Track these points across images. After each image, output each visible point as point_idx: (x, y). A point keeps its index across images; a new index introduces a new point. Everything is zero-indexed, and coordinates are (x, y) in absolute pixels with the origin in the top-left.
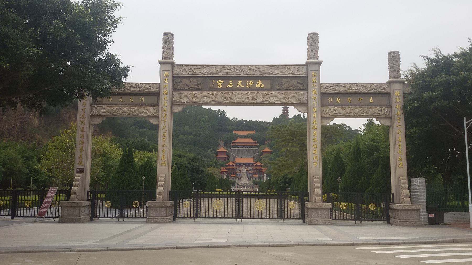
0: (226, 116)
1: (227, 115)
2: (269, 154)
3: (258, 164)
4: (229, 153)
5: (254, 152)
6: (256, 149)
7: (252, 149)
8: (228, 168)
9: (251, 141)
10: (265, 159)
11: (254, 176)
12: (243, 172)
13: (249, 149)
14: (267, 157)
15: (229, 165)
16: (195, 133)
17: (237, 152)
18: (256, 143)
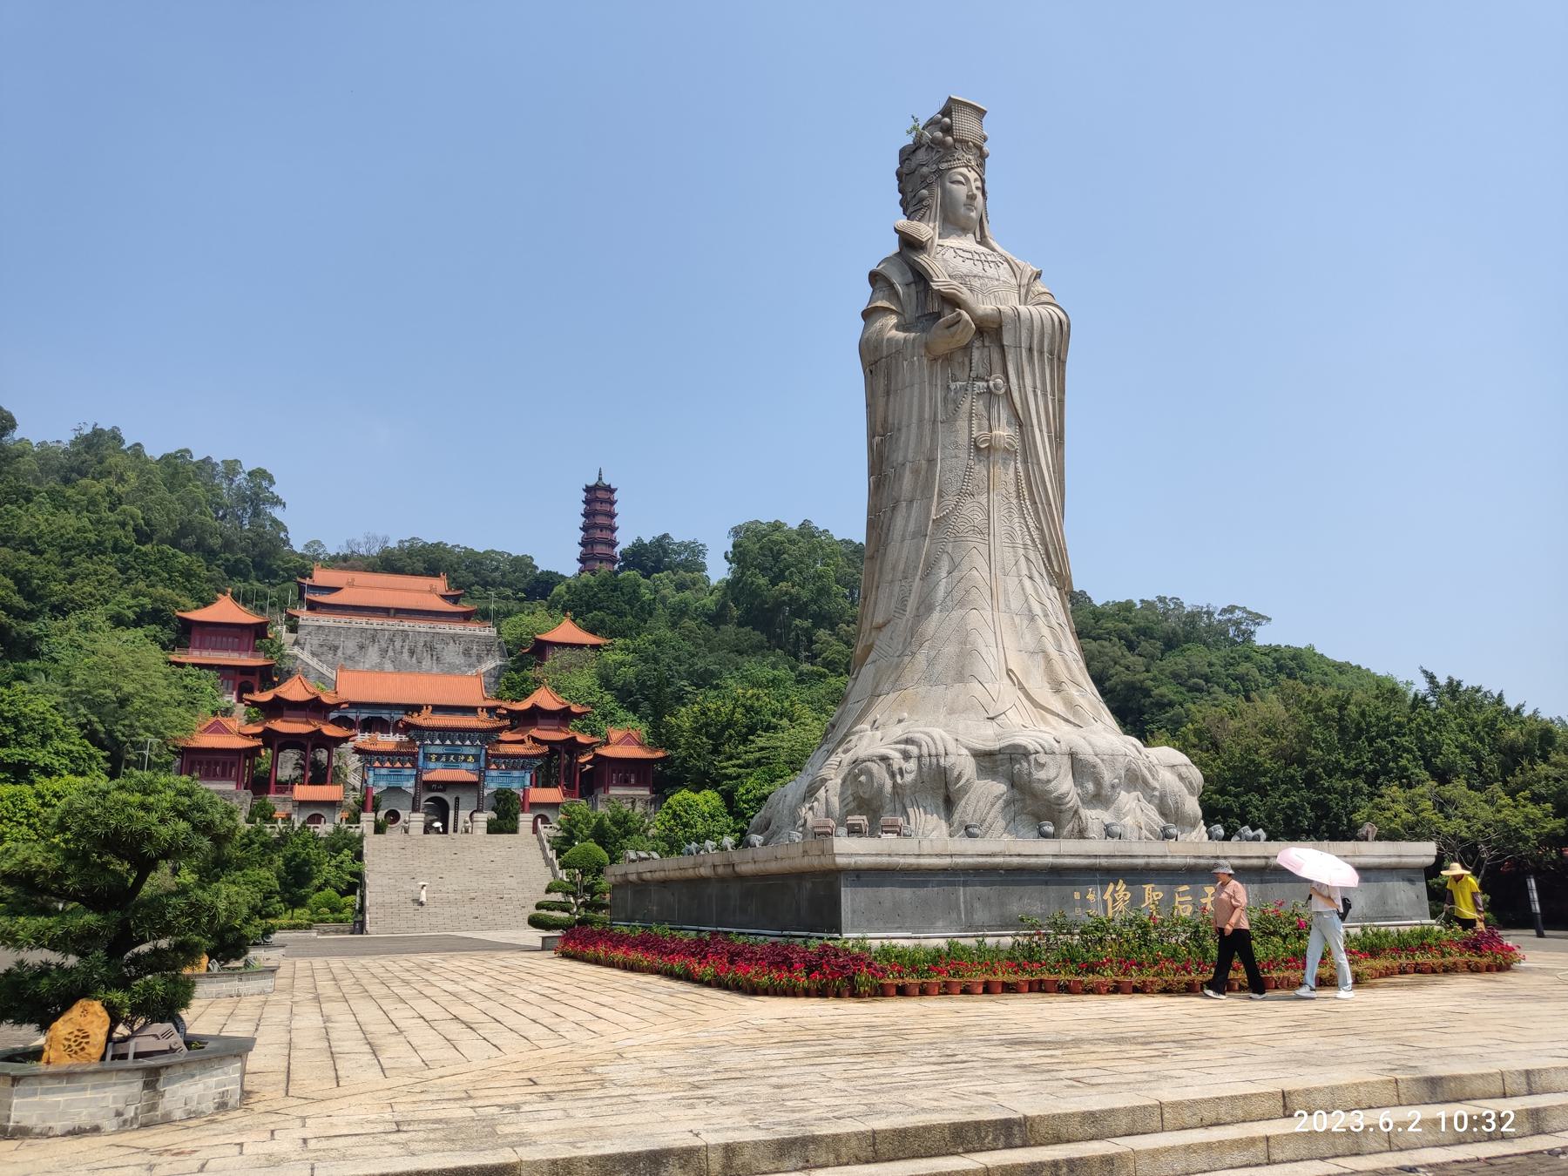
3: (545, 698)
5: (467, 653)
7: (454, 638)
12: (990, 330)
15: (278, 707)
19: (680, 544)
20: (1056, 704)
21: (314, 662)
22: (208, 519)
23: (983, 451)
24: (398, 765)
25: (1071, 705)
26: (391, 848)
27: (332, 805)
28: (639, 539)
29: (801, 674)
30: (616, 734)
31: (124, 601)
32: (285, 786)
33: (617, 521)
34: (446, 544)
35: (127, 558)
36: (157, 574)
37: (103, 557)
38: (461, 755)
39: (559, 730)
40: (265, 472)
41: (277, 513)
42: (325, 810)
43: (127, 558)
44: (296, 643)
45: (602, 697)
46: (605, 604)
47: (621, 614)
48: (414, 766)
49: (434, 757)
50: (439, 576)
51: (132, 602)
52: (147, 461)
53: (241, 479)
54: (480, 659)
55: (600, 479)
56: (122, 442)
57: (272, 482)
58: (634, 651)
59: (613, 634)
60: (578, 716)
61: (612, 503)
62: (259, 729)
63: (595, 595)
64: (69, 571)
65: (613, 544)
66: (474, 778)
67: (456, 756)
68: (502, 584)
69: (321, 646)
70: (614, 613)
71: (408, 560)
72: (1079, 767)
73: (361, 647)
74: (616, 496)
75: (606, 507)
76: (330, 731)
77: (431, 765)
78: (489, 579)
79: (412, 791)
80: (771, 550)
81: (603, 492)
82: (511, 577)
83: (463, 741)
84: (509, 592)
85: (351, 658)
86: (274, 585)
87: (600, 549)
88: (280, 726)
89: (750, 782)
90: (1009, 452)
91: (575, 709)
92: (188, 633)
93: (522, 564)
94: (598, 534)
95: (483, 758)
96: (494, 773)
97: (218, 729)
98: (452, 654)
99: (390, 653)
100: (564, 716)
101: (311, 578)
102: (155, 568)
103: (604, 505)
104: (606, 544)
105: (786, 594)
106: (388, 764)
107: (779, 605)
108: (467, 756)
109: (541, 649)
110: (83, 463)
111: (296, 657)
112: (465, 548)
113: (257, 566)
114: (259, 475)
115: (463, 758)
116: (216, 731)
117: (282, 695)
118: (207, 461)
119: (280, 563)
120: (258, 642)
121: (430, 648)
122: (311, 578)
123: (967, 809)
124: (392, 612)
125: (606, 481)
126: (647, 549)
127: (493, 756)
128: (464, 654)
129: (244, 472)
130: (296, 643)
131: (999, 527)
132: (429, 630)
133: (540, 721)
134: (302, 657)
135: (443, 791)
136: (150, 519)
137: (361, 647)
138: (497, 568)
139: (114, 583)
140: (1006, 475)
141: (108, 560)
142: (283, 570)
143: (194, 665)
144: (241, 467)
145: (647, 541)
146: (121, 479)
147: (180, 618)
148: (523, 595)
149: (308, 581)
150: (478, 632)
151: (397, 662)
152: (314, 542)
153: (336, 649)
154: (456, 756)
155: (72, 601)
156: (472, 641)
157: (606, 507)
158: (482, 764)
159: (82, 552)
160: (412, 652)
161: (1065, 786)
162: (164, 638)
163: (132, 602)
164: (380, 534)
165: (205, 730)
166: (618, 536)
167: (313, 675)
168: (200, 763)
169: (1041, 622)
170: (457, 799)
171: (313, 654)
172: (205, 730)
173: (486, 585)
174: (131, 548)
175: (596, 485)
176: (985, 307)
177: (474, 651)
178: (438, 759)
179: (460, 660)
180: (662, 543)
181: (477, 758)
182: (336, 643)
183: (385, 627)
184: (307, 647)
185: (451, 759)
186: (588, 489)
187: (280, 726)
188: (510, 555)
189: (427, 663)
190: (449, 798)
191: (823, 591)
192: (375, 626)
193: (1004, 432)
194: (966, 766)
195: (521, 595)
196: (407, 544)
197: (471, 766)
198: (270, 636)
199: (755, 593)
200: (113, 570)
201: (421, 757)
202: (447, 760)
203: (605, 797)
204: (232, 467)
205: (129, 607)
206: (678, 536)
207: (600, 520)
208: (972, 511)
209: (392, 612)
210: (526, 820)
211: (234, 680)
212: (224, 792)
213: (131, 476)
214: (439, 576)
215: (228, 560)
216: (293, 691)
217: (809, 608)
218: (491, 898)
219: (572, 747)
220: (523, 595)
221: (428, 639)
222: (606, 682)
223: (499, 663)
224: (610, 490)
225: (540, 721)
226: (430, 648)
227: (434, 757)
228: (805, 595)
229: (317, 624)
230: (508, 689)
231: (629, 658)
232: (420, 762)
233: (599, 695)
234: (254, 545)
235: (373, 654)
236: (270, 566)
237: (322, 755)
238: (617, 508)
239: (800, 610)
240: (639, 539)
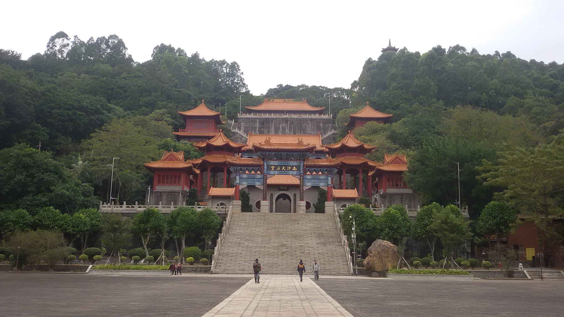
0: (241, 75)
1: (242, 73)
2: (382, 125)
4: (230, 130)
6: (326, 119)
7: (312, 120)
8: (204, 162)
9: (306, 107)
10: (367, 138)
13: (301, 120)
14: (375, 132)
15: (210, 149)
16: (124, 75)
17: (260, 128)
18: (320, 113)
24: (253, 172)
26: (245, 220)
38: (289, 166)
42: (226, 201)
48: (262, 173)
49: (273, 167)
52: (186, 57)
55: (390, 44)
56: (173, 49)
62: (200, 161)
66: (296, 181)
67: (286, 167)
77: (272, 172)
83: (317, 172)
95: (302, 168)
96: (309, 177)
100: (360, 150)
106: (247, 172)
108: (292, 167)
115: (290, 168)
125: (393, 45)
127: (307, 167)
134: (239, 133)
135: (287, 190)
147: (181, 115)
154: (286, 167)
158: (302, 172)
170: (295, 195)
178: (275, 169)
181: (298, 167)
185: (284, 170)
190: (290, 194)
197: (295, 173)
201: (265, 167)
202: (281, 169)
210: (329, 205)
218: (296, 253)
219: (366, 168)
227: (273, 167)
232: (265, 171)
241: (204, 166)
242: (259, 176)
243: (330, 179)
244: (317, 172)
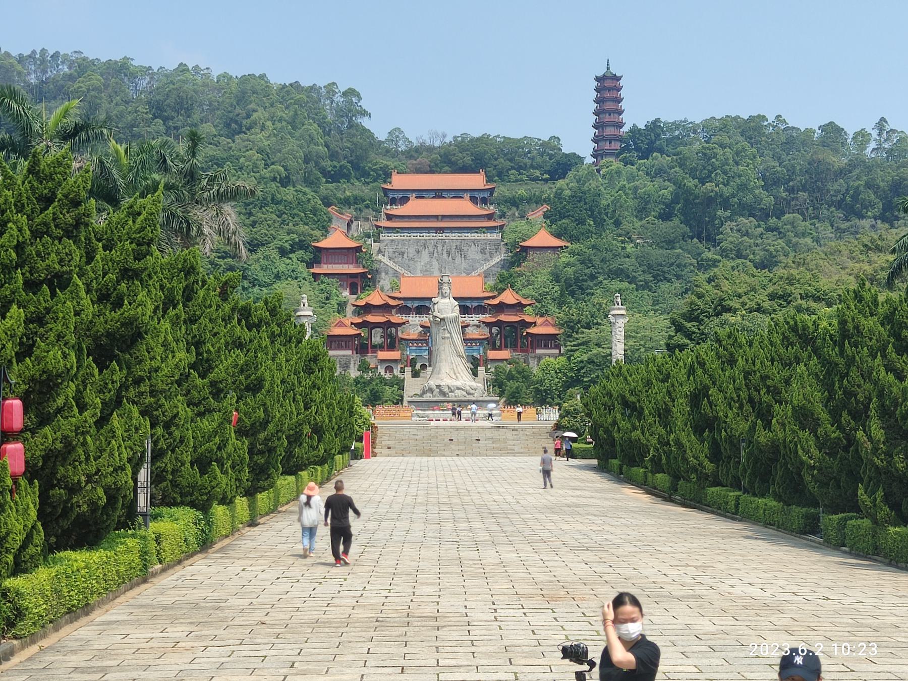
3: (509, 297)
5: (483, 251)
11: (492, 354)
12: (443, 319)
15: (368, 308)
19: (673, 124)
20: (455, 377)
21: (390, 264)
22: (321, 148)
23: (443, 338)
25: (457, 377)
27: (395, 361)
28: (634, 126)
29: (702, 260)
30: (539, 320)
31: (284, 239)
32: (376, 348)
33: (623, 105)
34: (489, 135)
35: (281, 207)
36: (298, 215)
37: (268, 208)
39: (516, 315)
40: (354, 90)
41: (365, 122)
43: (281, 207)
44: (380, 251)
45: (553, 288)
46: (571, 213)
47: (581, 222)
50: (479, 172)
51: (288, 238)
53: (338, 98)
54: (491, 255)
55: (608, 69)
57: (360, 98)
58: (578, 254)
59: (573, 239)
60: (529, 305)
61: (619, 89)
63: (564, 207)
64: (252, 218)
65: (620, 125)
68: (532, 167)
69: (394, 252)
70: (576, 220)
71: (460, 155)
72: (449, 388)
73: (418, 252)
74: (622, 82)
75: (613, 94)
76: (396, 318)
78: (522, 164)
79: (427, 357)
80: (705, 154)
81: (610, 81)
82: (538, 159)
84: (537, 173)
85: (412, 259)
86: (368, 183)
87: (609, 131)
88: (371, 318)
89: (577, 354)
90: (448, 338)
91: (524, 302)
92: (318, 256)
93: (550, 147)
94: (607, 118)
97: (341, 324)
98: (473, 253)
99: (436, 254)
100: (519, 307)
101: (390, 183)
102: (296, 211)
103: (611, 92)
104: (614, 126)
105: (712, 191)
107: (709, 201)
109: (525, 249)
110: (238, 115)
111: (380, 261)
112: (504, 137)
113: (356, 166)
114: (350, 93)
116: (340, 326)
117: (369, 302)
118: (312, 88)
119: (370, 165)
120: (358, 254)
121: (459, 250)
122: (390, 183)
123: (434, 393)
124: (440, 218)
125: (613, 70)
126: (641, 134)
128: (481, 253)
129: (340, 91)
130: (380, 251)
131: (447, 349)
132: (458, 238)
133: (505, 310)
134: (383, 261)
136: (287, 166)
137: (418, 252)
138: (529, 152)
139: (276, 225)
140: (448, 341)
141: (271, 210)
142: (373, 170)
143: (325, 274)
144: (337, 88)
145: (642, 126)
146: (263, 128)
147: (314, 246)
148: (547, 176)
149: (388, 186)
150: (489, 237)
151: (440, 261)
152: (395, 130)
153: (403, 253)
155: (256, 239)
156: (486, 243)
157: (613, 94)
159: (256, 205)
160: (449, 254)
161: (446, 390)
162: (306, 258)
163: (288, 238)
164: (440, 133)
165: (335, 326)
166: (624, 117)
167: (391, 271)
168: (335, 342)
169: (454, 364)
171: (390, 259)
172: (335, 326)
173: (520, 168)
174: (281, 201)
175: (604, 75)
176: (442, 317)
177: (487, 251)
179: (479, 256)
180: (655, 127)
182: (403, 250)
183: (431, 238)
184: (386, 254)
186: (598, 79)
187: (371, 318)
188: (539, 140)
189: (458, 260)
191: (743, 187)
192: (425, 238)
193: (448, 335)
194: (435, 387)
195: (546, 176)
196: (460, 139)
198: (364, 250)
199: (688, 192)
200: (274, 217)
203: (533, 355)
204: (331, 88)
205: (286, 241)
206: (668, 117)
207: (609, 106)
208: (442, 348)
209: (440, 218)
211: (347, 281)
212: (347, 356)
213: (269, 123)
214: (479, 172)
215: (335, 167)
216: (375, 298)
217: (731, 200)
219: (525, 324)
220: (547, 176)
221: (458, 244)
222: (556, 278)
223: (503, 257)
224: (617, 79)
225: (505, 310)
226: (459, 250)
228: (727, 191)
229: (391, 238)
230: (501, 282)
231: (572, 260)
233: (551, 287)
234: (352, 151)
235: (425, 254)
236: (364, 167)
237: (393, 330)
238: (623, 93)
239: (726, 204)
240: (634, 126)
241: (364, 324)
242: (424, 348)
243: (481, 349)
244: (471, 344)
